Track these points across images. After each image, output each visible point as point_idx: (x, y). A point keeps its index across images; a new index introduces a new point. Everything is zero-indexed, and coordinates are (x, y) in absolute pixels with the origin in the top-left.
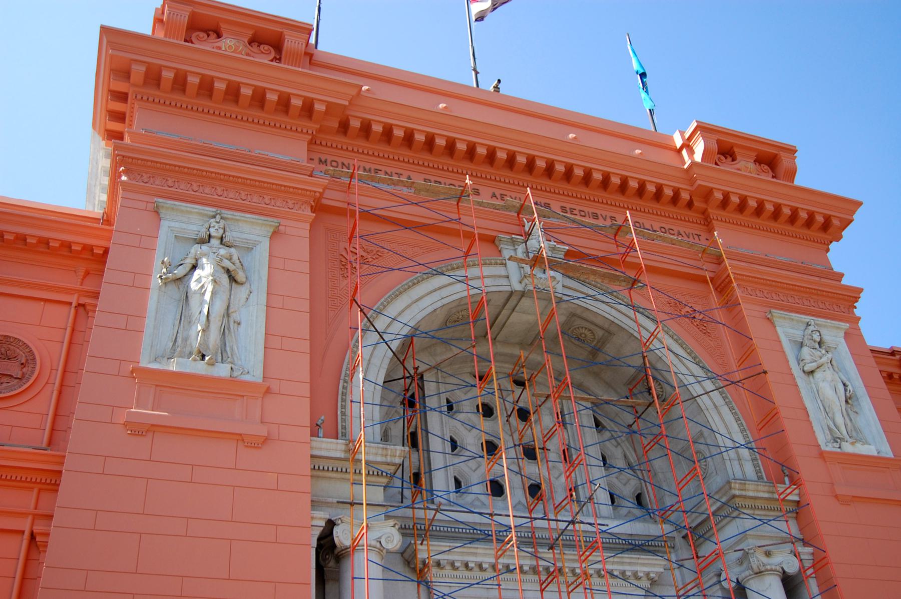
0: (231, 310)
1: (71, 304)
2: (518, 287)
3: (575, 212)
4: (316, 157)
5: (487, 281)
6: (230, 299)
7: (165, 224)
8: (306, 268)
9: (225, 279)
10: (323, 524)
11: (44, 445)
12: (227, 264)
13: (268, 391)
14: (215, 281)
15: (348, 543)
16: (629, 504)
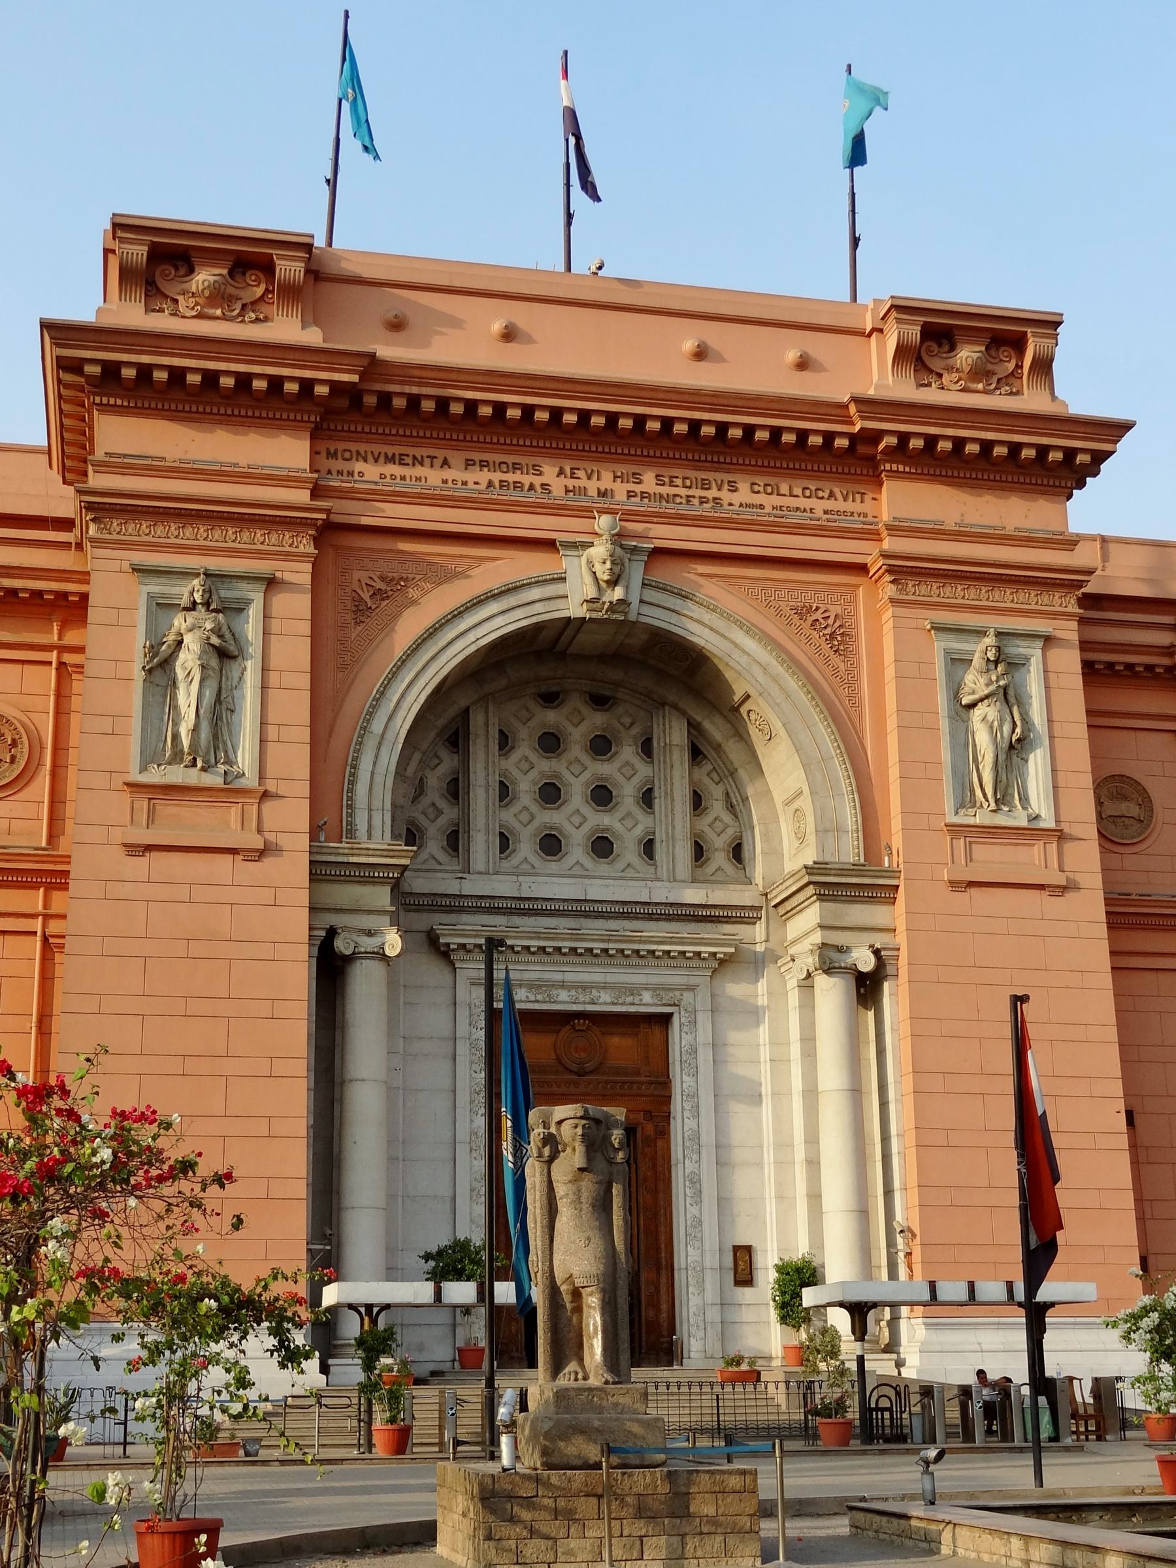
0: (224, 695)
1: (50, 663)
3: (679, 482)
4: (322, 446)
5: (538, 608)
6: (220, 682)
7: (146, 589)
8: (305, 628)
9: (214, 662)
10: (324, 933)
11: (44, 845)
12: (215, 640)
13: (265, 795)
14: (203, 667)
15: (348, 952)
16: (719, 859)
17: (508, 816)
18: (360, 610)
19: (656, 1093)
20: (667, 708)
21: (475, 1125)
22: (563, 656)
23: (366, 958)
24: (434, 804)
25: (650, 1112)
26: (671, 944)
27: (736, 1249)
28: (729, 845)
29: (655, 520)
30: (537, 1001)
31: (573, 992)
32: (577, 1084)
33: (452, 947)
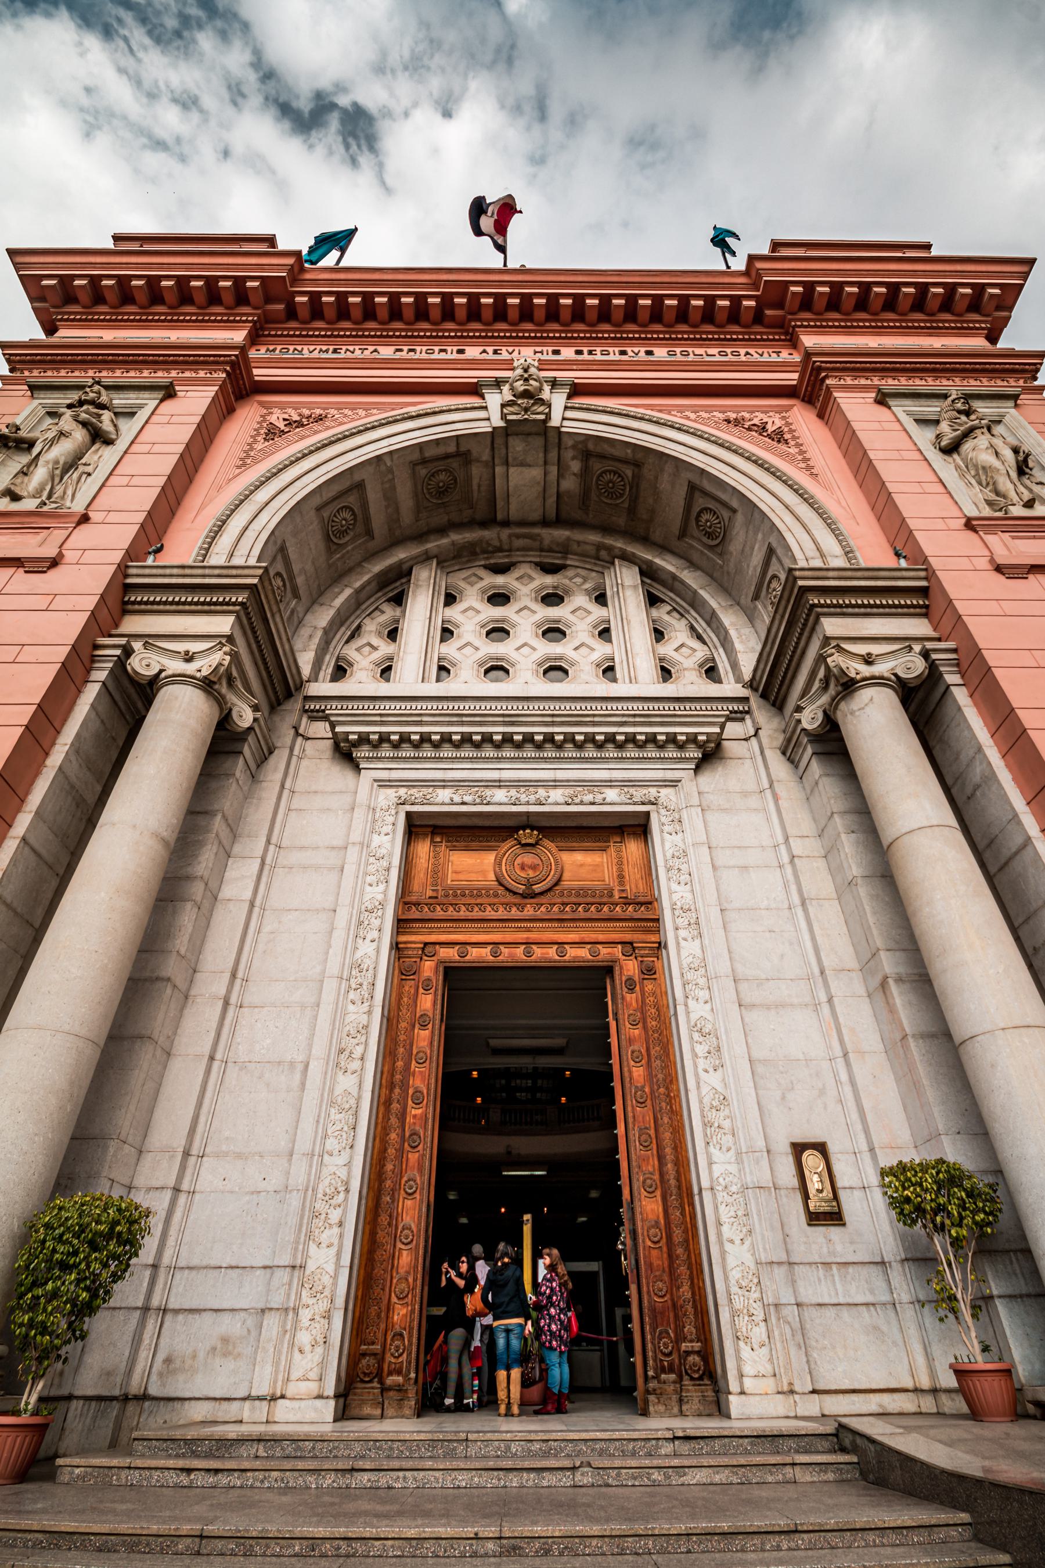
2: (497, 422)
17: (450, 649)
18: (272, 433)
19: (636, 915)
20: (617, 561)
21: (359, 954)
22: (506, 523)
23: (173, 683)
24: (369, 644)
25: (631, 943)
26: (635, 724)
27: (799, 1149)
28: (701, 666)
29: (575, 367)
30: (463, 803)
31: (513, 792)
32: (521, 907)
33: (351, 737)
